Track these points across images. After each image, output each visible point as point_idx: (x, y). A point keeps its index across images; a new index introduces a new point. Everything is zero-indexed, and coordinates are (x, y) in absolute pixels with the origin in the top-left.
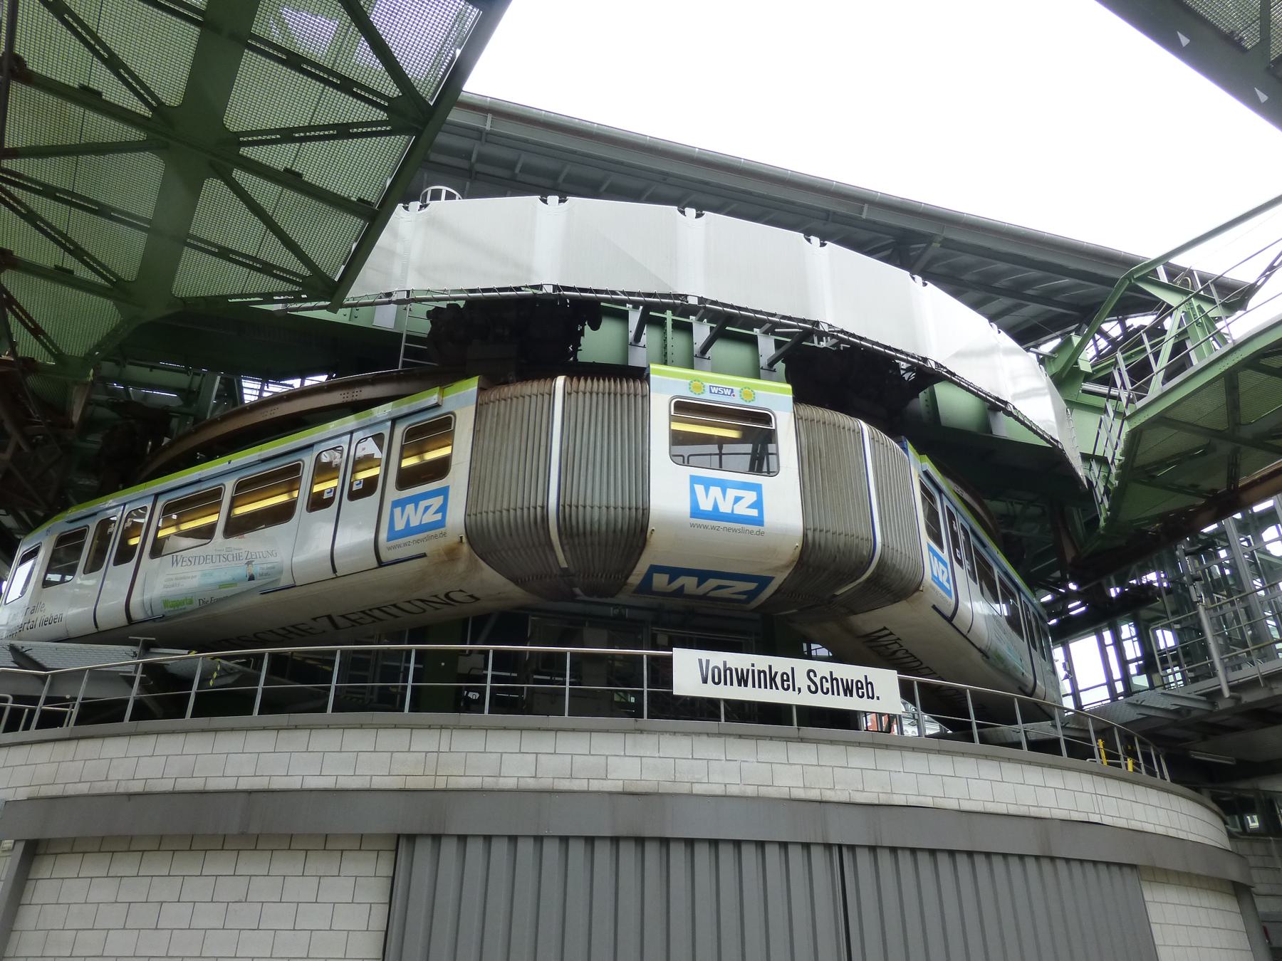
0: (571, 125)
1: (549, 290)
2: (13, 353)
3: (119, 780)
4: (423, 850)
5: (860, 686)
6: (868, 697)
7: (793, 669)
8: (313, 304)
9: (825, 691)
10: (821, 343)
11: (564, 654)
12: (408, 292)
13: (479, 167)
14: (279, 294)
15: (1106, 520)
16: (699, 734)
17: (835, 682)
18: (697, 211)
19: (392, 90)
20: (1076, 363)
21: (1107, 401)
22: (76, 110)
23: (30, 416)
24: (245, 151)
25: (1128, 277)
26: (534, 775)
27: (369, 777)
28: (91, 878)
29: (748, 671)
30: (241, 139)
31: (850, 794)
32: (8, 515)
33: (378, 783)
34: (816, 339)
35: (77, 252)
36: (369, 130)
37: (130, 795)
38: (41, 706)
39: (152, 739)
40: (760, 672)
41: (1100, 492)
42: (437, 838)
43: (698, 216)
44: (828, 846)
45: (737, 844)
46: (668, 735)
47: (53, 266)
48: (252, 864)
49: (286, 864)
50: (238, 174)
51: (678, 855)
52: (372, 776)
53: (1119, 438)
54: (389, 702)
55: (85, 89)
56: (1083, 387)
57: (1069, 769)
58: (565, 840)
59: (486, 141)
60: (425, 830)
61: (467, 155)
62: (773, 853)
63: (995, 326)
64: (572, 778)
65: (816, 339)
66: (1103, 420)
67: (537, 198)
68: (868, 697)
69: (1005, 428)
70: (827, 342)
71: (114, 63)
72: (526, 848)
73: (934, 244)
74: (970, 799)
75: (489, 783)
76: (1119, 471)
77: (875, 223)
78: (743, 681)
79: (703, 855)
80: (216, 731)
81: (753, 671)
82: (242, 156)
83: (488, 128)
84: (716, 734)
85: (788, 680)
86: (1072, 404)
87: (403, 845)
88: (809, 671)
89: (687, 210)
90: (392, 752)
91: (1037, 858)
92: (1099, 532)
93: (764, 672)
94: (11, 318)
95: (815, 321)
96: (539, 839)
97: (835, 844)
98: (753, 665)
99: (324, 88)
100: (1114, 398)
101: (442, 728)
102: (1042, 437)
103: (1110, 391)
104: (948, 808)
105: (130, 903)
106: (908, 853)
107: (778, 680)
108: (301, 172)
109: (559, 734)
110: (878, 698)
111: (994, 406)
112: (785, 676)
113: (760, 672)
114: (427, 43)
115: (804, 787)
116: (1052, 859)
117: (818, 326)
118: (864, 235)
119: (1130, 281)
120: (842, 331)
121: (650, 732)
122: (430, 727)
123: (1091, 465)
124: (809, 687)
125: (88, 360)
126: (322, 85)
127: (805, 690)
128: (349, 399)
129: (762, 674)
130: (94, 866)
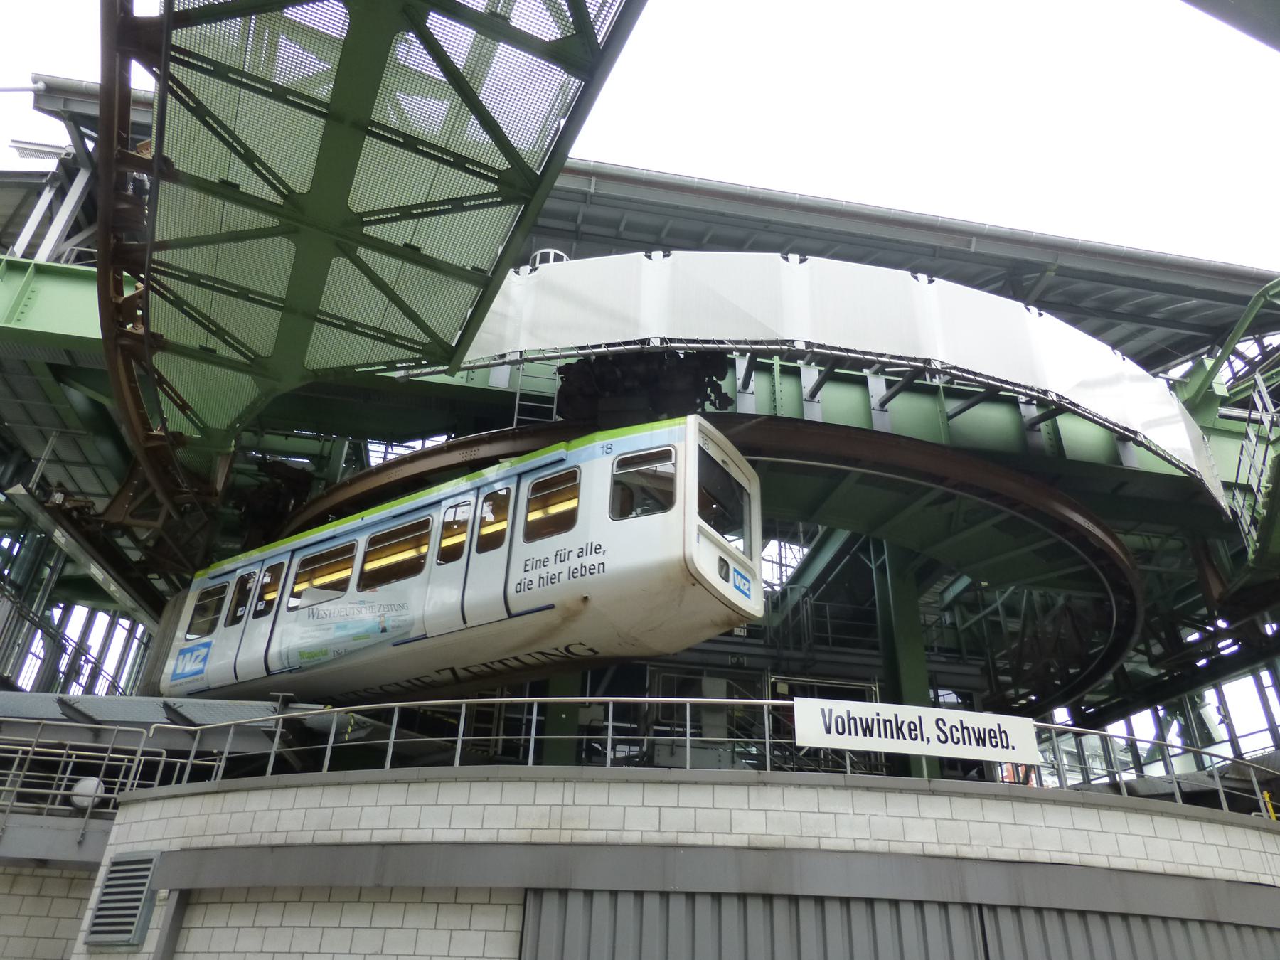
0: (673, 181)
1: (656, 343)
2: (164, 428)
3: (262, 832)
4: (551, 904)
5: (993, 735)
6: (1003, 747)
7: (920, 718)
8: (432, 369)
9: (956, 740)
10: (934, 380)
11: (683, 706)
12: (521, 352)
13: (584, 228)
14: (401, 361)
15: (1255, 552)
16: (824, 786)
17: (965, 731)
18: (800, 256)
19: (501, 163)
20: (1211, 387)
21: (1248, 425)
22: (216, 203)
23: (178, 485)
24: (368, 230)
25: (1263, 294)
26: (658, 829)
27: (496, 831)
28: (239, 927)
29: (873, 720)
30: (364, 219)
31: (988, 850)
32: (160, 578)
33: (506, 836)
34: (928, 377)
35: (219, 332)
36: (481, 202)
37: (273, 847)
38: (191, 761)
39: (292, 792)
40: (885, 721)
41: (1246, 523)
42: (564, 893)
43: (802, 261)
44: (967, 906)
45: (870, 902)
46: (792, 788)
47: (198, 346)
48: (386, 917)
49: (418, 918)
50: (362, 252)
51: (808, 912)
52: (499, 829)
53: (1264, 464)
54: (513, 755)
55: (224, 183)
56: (1220, 412)
57: (1232, 824)
58: (691, 896)
59: (591, 203)
60: (552, 886)
61: (573, 218)
62: (908, 912)
63: (1119, 354)
64: (695, 832)
65: (928, 377)
66: (1245, 445)
67: (642, 254)
68: (1003, 747)
69: (1136, 459)
70: (940, 378)
71: (249, 157)
72: (652, 904)
73: (1048, 273)
74: (1121, 856)
75: (614, 837)
76: (1266, 499)
77: (984, 255)
78: (868, 731)
79: (834, 913)
80: (351, 784)
81: (878, 720)
82: (365, 235)
83: (592, 190)
84: (842, 786)
85: (915, 730)
86: (1209, 431)
87: (530, 898)
88: (938, 720)
89: (791, 256)
90: (518, 806)
91: (1202, 922)
92: (1248, 566)
93: (890, 721)
94: (162, 397)
95: (927, 359)
96: (665, 895)
97: (974, 904)
98: (878, 714)
99: (439, 166)
100: (1255, 421)
101: (565, 781)
102: (1178, 467)
103: (1250, 414)
104: (1096, 865)
105: (274, 953)
106: (1055, 914)
107: (905, 729)
108: (419, 246)
109: (681, 786)
110: (1013, 748)
111: (1122, 437)
112: (912, 725)
113: (885, 721)
114: (533, 116)
115: (939, 843)
116: (1220, 924)
117: (929, 364)
118: (974, 269)
119: (1265, 298)
120: (955, 368)
121: (773, 784)
122: (553, 781)
123: (1234, 495)
124: (938, 737)
125: (231, 431)
126: (437, 164)
127: (934, 740)
128: (468, 458)
129: (888, 724)
130: (241, 917)
